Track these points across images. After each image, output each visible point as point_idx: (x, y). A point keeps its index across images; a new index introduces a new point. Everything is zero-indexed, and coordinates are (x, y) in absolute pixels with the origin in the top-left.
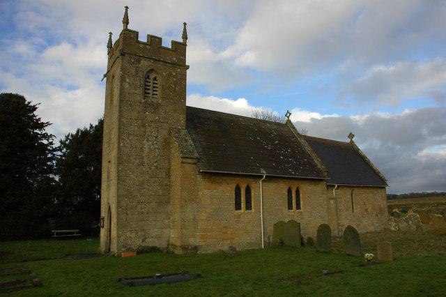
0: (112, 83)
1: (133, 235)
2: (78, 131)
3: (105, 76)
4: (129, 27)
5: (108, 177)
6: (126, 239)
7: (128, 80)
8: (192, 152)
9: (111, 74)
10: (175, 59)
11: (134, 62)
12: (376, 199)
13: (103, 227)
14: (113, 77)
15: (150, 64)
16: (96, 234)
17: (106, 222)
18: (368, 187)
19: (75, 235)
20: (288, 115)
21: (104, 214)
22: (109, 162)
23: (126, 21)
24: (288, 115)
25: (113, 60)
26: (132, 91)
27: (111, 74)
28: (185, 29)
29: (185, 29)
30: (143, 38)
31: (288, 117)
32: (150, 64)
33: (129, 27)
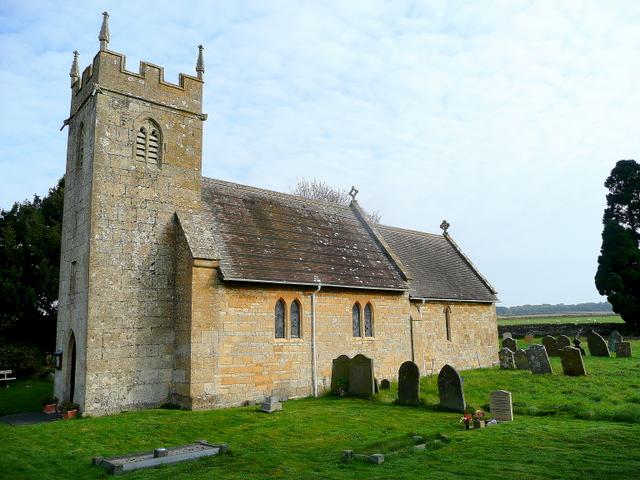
0: (80, 135)
1: (113, 381)
2: (15, 206)
3: (67, 122)
4: (110, 47)
5: (72, 287)
6: (101, 388)
7: (108, 134)
8: (211, 250)
9: (78, 121)
10: (184, 103)
11: (118, 106)
12: (484, 321)
13: (60, 368)
14: (82, 125)
15: (145, 109)
16: (46, 377)
17: (66, 361)
18: (470, 304)
19: (6, 379)
20: (353, 192)
21: (62, 346)
22: (74, 263)
23: (103, 39)
24: (353, 192)
25: (81, 98)
26: (114, 152)
27: (78, 121)
28: (105, 22)
29: (105, 22)
30: (132, 67)
31: (353, 196)
32: (145, 109)
33: (110, 47)
